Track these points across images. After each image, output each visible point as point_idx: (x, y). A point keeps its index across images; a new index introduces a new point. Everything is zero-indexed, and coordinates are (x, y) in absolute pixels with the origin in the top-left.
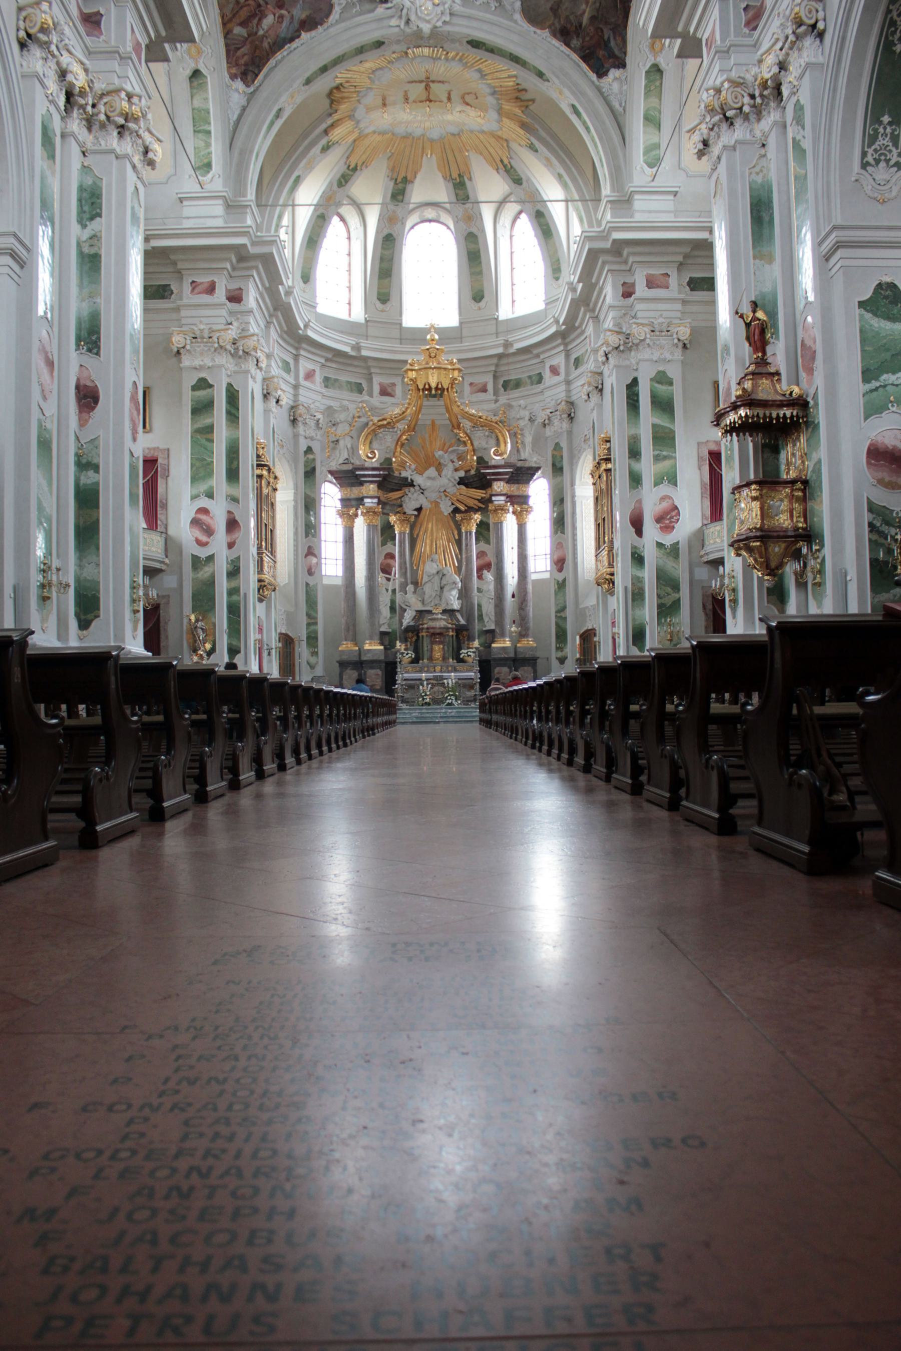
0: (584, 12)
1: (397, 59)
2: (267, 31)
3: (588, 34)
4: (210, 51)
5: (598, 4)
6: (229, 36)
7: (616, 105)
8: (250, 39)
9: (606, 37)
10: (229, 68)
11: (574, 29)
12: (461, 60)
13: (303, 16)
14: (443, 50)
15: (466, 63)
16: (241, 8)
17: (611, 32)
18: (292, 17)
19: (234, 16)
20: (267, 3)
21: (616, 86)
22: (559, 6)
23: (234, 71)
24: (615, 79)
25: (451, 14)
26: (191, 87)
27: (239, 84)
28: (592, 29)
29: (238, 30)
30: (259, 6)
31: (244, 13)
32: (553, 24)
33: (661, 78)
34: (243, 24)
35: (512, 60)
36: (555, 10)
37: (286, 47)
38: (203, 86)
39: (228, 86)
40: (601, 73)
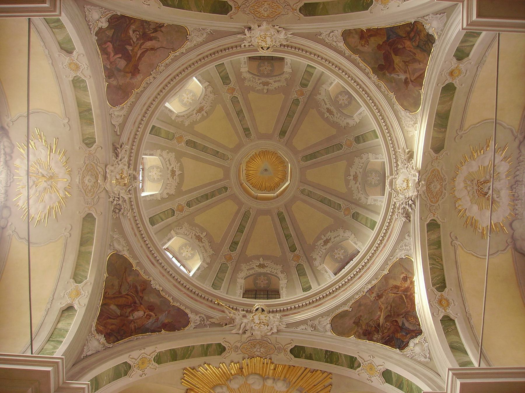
0: (380, 316)
1: (235, 376)
2: (136, 319)
3: (386, 328)
4: (86, 294)
5: (389, 308)
6: (106, 307)
7: (423, 359)
8: (121, 318)
9: (400, 324)
10: (97, 324)
11: (374, 329)
12: (283, 380)
13: (166, 321)
14: (273, 363)
15: (290, 383)
16: (121, 297)
17: (404, 319)
18: (158, 319)
19: (114, 298)
20: (141, 304)
21: (417, 349)
22: (360, 319)
23: (101, 328)
24: (416, 344)
25: (278, 331)
26: (61, 316)
27: (102, 339)
28: (388, 324)
29: (113, 307)
30: (135, 303)
31: (122, 301)
32: (357, 331)
33: (455, 324)
34: (118, 306)
35: (327, 362)
36: (357, 323)
37: (147, 334)
38: (71, 317)
39: (91, 332)
40: (402, 346)
